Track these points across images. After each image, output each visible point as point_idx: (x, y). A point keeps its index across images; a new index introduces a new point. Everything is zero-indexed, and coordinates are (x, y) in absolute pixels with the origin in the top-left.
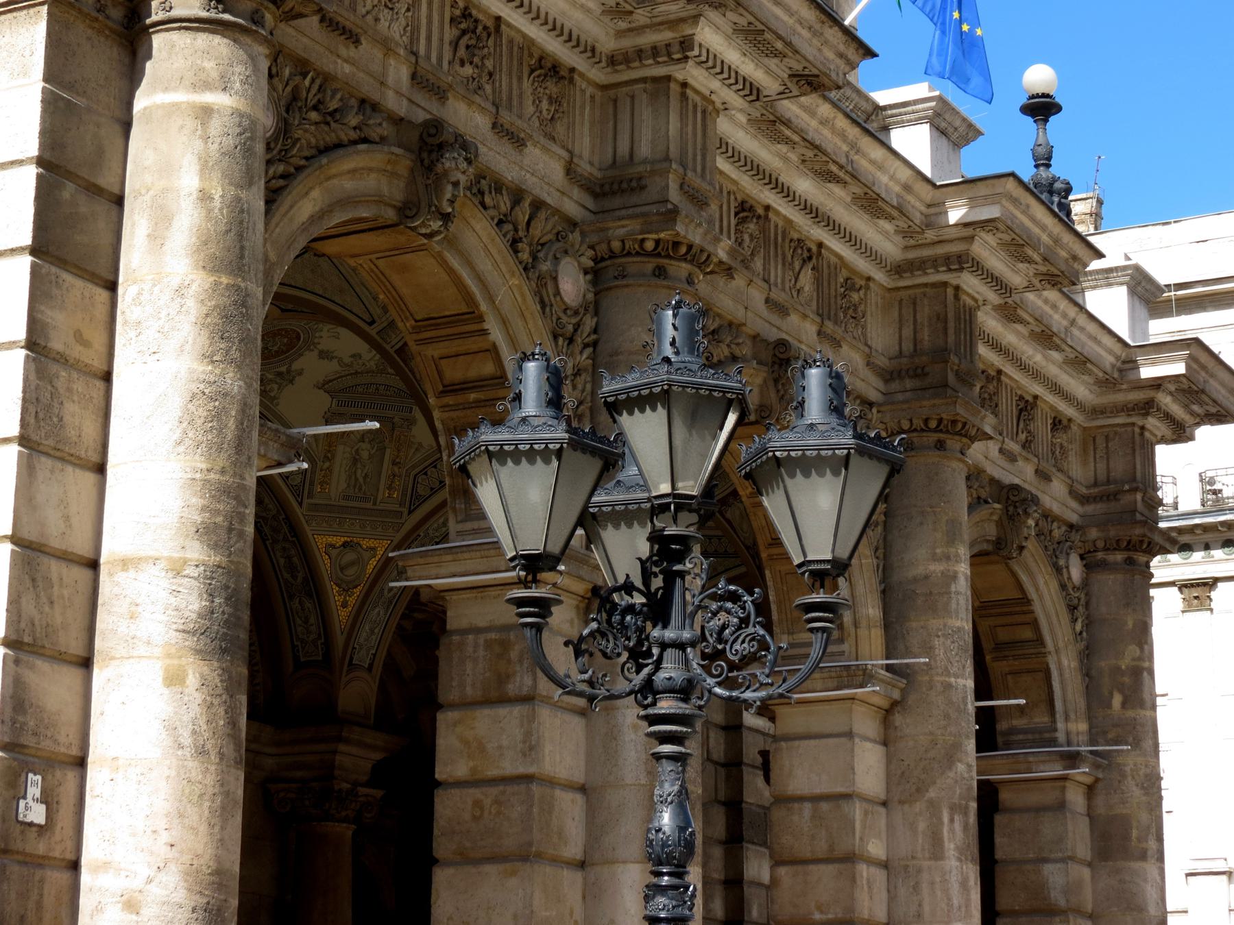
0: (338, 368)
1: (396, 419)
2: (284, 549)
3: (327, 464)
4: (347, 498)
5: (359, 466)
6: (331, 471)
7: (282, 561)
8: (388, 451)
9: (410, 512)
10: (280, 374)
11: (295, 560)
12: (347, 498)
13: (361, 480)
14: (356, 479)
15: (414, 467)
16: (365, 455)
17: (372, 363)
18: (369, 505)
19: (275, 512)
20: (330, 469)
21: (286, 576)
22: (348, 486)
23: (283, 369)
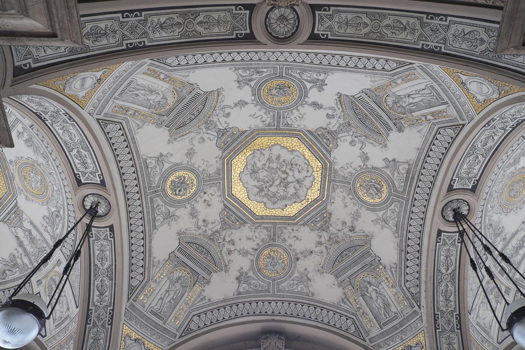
0: (225, 103)
1: (165, 118)
2: (114, 32)
3: (162, 76)
4: (131, 82)
5: (147, 92)
6: (156, 78)
7: (102, 25)
8: (146, 110)
9: (98, 120)
10: (251, 80)
11: (105, 41)
12: (131, 82)
13: (137, 92)
14: (138, 90)
15: (127, 123)
16: (152, 97)
17: (215, 120)
18: (116, 95)
19: (151, 36)
20: (158, 77)
21: (89, 26)
22: (137, 85)
23: (252, 83)
